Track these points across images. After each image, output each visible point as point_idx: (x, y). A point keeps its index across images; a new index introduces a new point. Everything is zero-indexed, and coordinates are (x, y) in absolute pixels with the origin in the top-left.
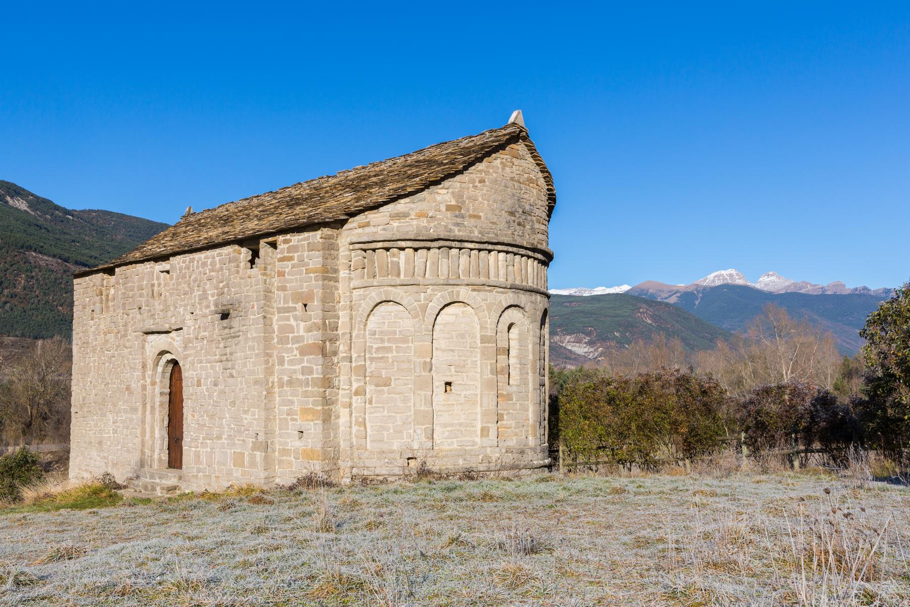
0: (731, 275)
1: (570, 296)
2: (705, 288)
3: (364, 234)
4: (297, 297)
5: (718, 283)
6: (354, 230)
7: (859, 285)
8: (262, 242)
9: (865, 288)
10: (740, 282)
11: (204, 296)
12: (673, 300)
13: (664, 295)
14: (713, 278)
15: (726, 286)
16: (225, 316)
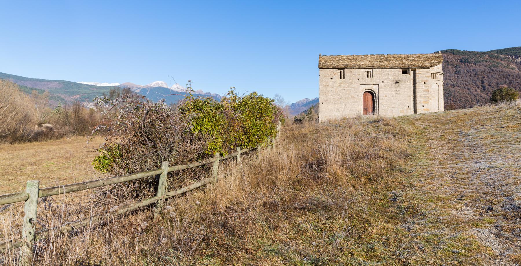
0: (162, 83)
1: (91, 85)
2: (151, 88)
3: (433, 71)
4: (422, 81)
5: (156, 86)
6: (430, 70)
7: (208, 92)
8: (410, 69)
9: (209, 93)
10: (165, 86)
11: (388, 78)
12: (137, 91)
13: (134, 89)
14: (155, 83)
15: (160, 87)
16: (397, 82)
